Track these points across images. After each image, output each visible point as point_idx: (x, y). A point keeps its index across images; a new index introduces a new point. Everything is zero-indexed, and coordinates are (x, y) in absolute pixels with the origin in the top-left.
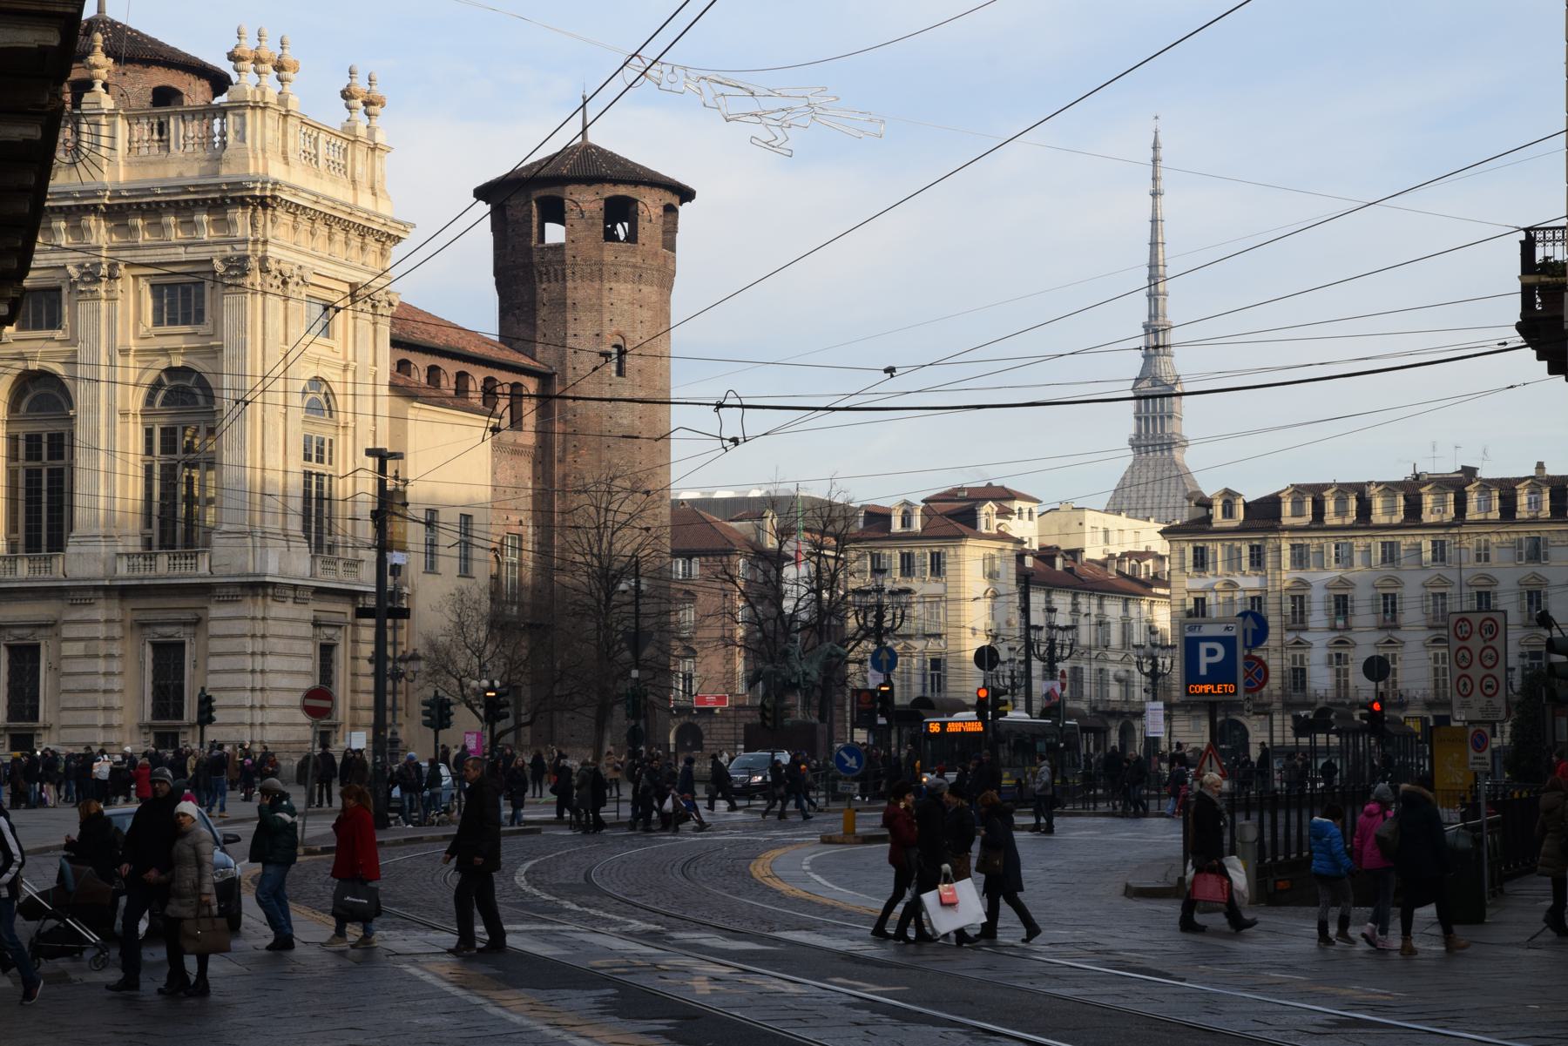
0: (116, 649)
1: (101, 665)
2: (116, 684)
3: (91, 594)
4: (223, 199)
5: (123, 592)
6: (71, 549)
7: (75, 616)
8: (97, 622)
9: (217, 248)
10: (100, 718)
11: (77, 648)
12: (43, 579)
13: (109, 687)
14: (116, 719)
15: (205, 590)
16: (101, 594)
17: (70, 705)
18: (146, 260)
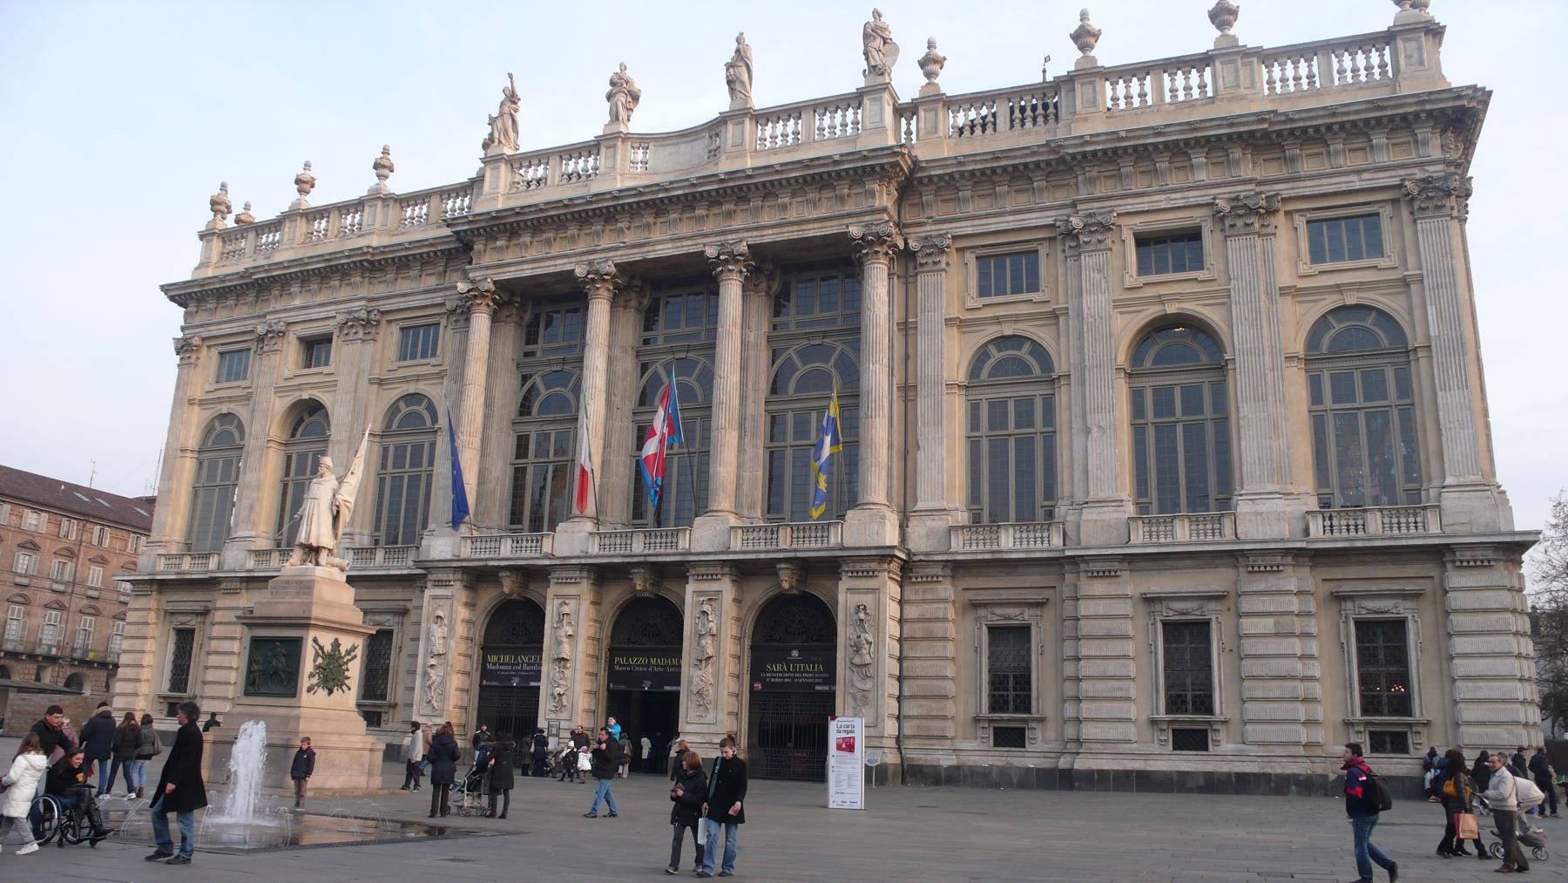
0: (1312, 626)
1: (1297, 646)
2: (1315, 669)
3: (1278, 560)
4: (1417, 115)
5: (1317, 557)
6: (1243, 507)
7: (1260, 584)
8: (1288, 593)
9: (1403, 172)
10: (1301, 712)
11: (1267, 624)
12: (1210, 541)
13: (1309, 673)
14: (1319, 712)
15: (1439, 554)
16: (1289, 559)
17: (1260, 694)
18: (1308, 192)
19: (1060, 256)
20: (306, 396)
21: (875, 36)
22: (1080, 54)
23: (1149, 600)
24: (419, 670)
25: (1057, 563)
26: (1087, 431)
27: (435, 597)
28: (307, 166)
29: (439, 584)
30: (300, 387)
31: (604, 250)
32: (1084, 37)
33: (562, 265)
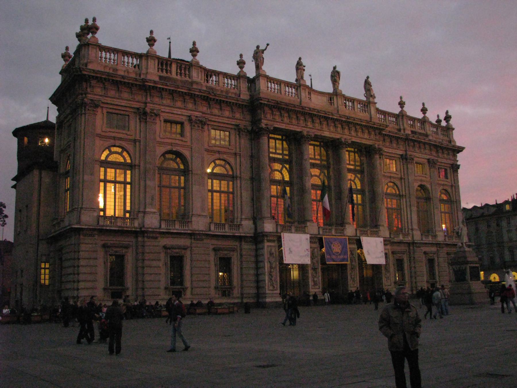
6: (437, 233)
19: (402, 164)
20: (174, 150)
21: (367, 84)
22: (400, 109)
23: (425, 253)
24: (267, 274)
25: (409, 244)
26: (411, 211)
27: (268, 246)
28: (151, 32)
29: (269, 241)
30: (171, 144)
31: (309, 128)
32: (402, 104)
33: (299, 130)
